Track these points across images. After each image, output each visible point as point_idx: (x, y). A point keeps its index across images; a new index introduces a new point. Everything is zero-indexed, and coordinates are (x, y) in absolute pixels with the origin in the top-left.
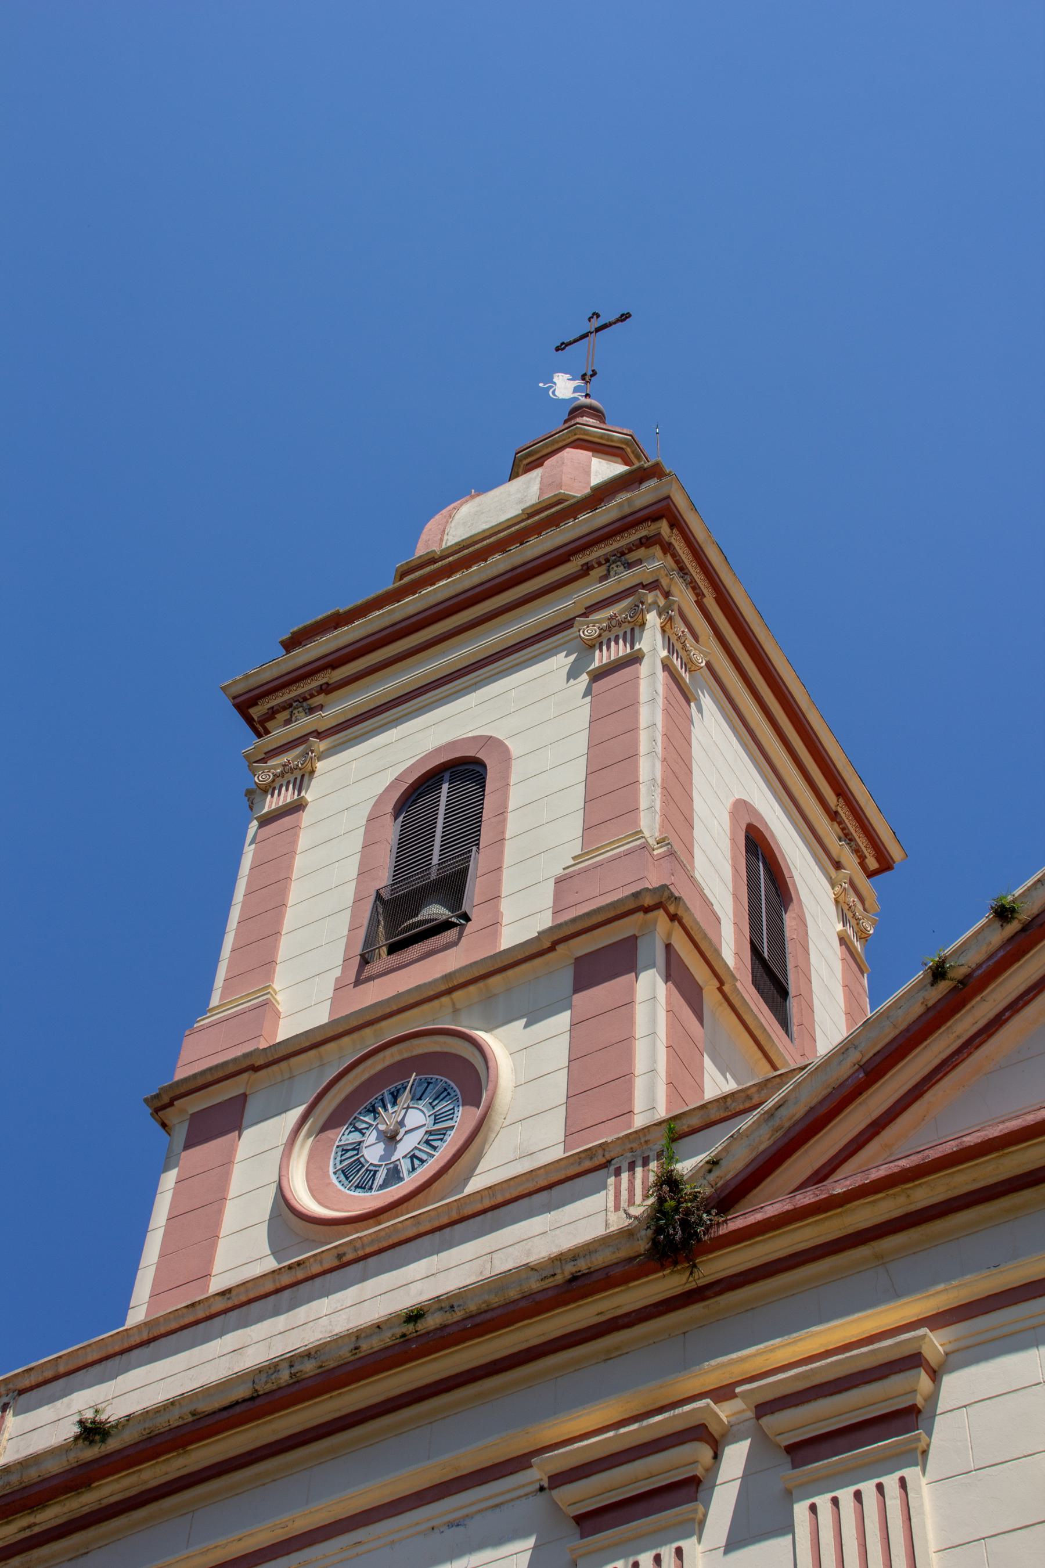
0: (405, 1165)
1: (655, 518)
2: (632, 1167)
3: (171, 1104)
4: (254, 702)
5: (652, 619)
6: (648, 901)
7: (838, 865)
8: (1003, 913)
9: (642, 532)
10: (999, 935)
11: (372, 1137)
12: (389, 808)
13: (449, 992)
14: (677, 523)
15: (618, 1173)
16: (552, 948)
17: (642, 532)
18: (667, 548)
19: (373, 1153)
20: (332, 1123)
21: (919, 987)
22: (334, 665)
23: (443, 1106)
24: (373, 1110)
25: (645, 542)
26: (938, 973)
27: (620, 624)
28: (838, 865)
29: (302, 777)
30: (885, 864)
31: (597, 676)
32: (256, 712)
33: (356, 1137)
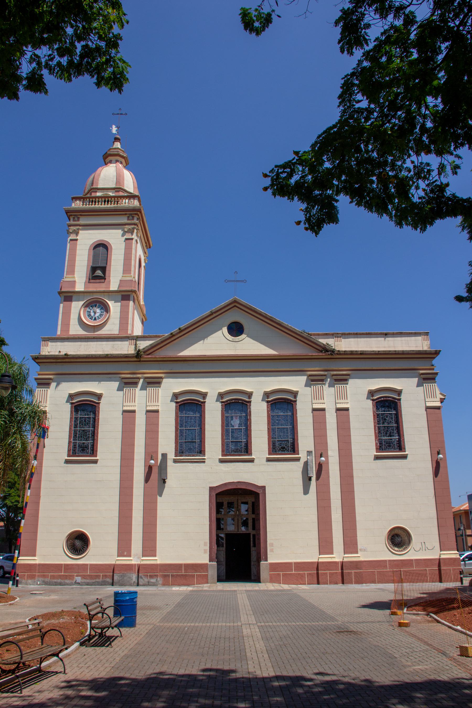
0: (97, 318)
1: (138, 211)
2: (132, 340)
3: (61, 293)
4: (69, 212)
5: (135, 231)
6: (133, 291)
7: (145, 253)
8: (179, 329)
9: (135, 213)
10: (178, 331)
11: (92, 311)
12: (92, 248)
13: (104, 292)
14: (141, 212)
15: (130, 340)
16: (119, 292)
17: (135, 213)
18: (138, 215)
19: (92, 314)
20: (87, 306)
21: (169, 335)
22: (83, 212)
23: (102, 311)
24: (92, 306)
25: (135, 214)
26: (172, 334)
27: (131, 230)
28: (145, 253)
29: (77, 234)
30: (150, 247)
31: (127, 239)
32: (68, 214)
33: (89, 310)
